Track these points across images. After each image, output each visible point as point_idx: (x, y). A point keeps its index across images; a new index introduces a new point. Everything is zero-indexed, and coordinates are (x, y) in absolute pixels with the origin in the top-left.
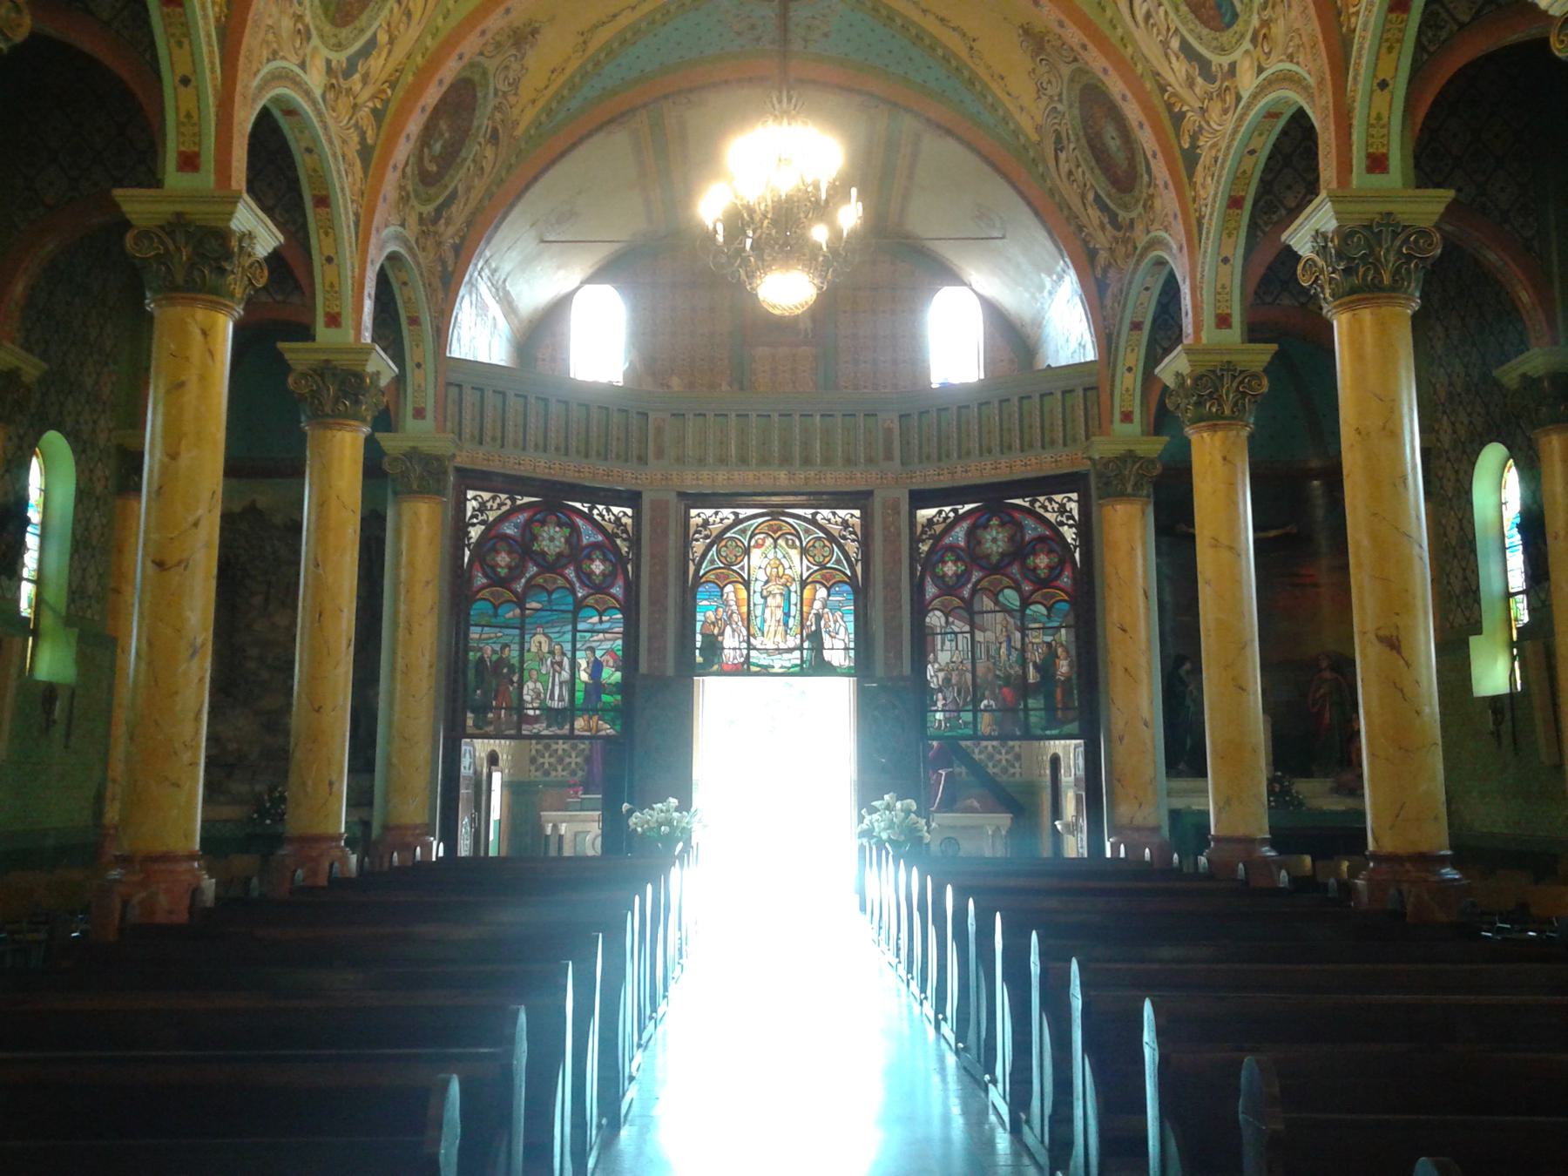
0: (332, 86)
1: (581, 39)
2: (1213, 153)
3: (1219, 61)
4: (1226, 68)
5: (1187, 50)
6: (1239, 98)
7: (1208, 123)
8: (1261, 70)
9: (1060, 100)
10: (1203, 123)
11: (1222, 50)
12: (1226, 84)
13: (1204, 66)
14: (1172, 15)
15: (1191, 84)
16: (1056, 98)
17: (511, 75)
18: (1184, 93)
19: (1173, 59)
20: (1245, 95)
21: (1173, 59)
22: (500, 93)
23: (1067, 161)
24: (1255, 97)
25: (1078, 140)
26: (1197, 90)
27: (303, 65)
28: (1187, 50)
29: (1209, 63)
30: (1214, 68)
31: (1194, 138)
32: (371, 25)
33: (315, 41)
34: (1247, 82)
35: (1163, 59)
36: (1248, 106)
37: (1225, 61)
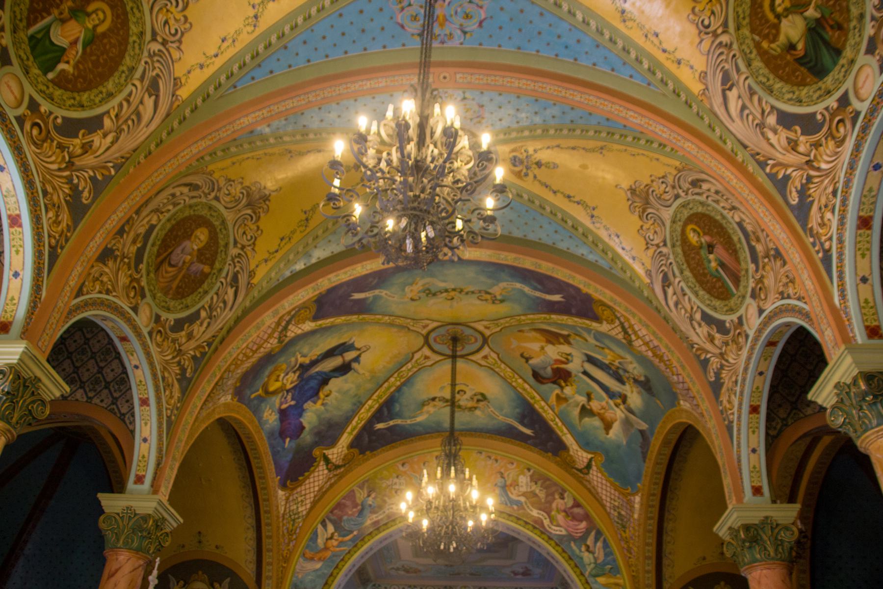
0: (160, 332)
1: (304, 217)
2: (734, 379)
3: (729, 319)
4: (736, 320)
5: (707, 319)
6: (747, 336)
7: (727, 361)
8: (761, 311)
9: (665, 245)
10: (724, 362)
11: (731, 310)
12: (738, 331)
13: (721, 327)
14: (693, 298)
15: (711, 339)
16: (661, 244)
17: (250, 234)
18: (708, 346)
19: (696, 326)
20: (751, 334)
21: (696, 326)
22: (239, 246)
23: (675, 294)
24: (760, 331)
25: (682, 272)
26: (716, 342)
27: (135, 309)
28: (707, 319)
29: (724, 322)
30: (728, 325)
31: (718, 374)
32: (193, 306)
33: (149, 299)
34: (753, 322)
35: (690, 327)
36: (756, 339)
37: (734, 317)
